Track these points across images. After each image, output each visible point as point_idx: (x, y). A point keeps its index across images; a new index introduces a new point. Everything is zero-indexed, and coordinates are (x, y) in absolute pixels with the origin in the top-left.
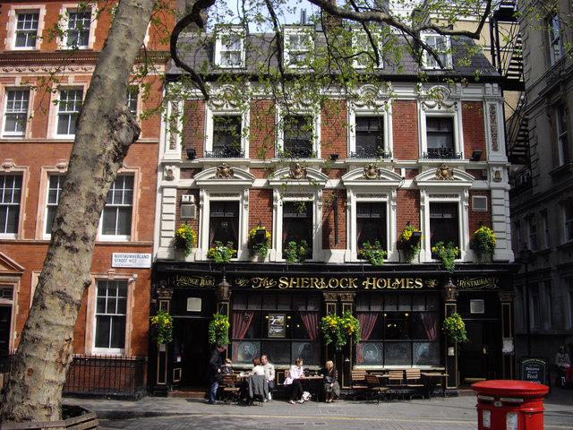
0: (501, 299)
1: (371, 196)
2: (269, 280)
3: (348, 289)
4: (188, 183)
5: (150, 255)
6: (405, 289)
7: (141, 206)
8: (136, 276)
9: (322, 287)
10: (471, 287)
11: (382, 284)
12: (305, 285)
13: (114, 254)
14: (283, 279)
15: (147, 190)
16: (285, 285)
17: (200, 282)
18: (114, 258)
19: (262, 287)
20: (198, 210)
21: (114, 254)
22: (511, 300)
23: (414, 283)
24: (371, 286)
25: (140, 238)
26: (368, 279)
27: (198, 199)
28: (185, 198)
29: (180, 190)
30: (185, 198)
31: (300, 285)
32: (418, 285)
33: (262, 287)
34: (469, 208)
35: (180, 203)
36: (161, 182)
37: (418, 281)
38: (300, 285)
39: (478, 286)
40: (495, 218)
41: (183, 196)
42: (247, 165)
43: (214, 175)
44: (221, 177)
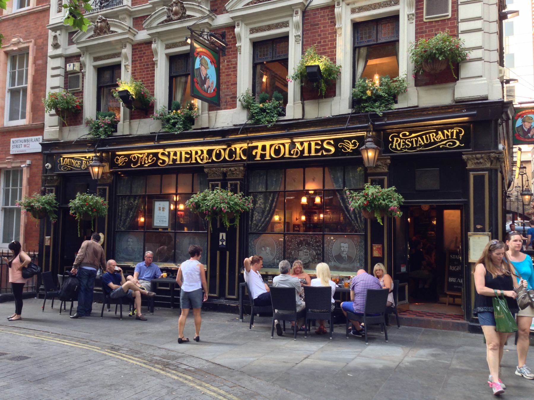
0: (470, 166)
1: (269, 28)
2: (148, 156)
3: (234, 161)
4: (73, 49)
5: (41, 137)
6: (309, 157)
7: (34, 83)
8: (28, 162)
9: (205, 161)
10: (412, 148)
11: (277, 152)
12: (187, 159)
13: (12, 140)
14: (163, 154)
15: (39, 65)
16: (164, 161)
17: (81, 164)
18: (12, 144)
19: (142, 166)
20: (83, 78)
21: (12, 140)
22: (488, 165)
23: (323, 148)
24: (263, 156)
25: (34, 119)
26: (260, 148)
27: (82, 66)
28: (70, 67)
29: (69, 59)
30: (70, 67)
31: (181, 160)
32: (328, 151)
33: (142, 166)
34: (418, 15)
35: (67, 74)
36: (51, 51)
37: (329, 143)
38: (181, 160)
39: (426, 145)
40: (462, 27)
41: (68, 65)
42: (129, 13)
43: (92, 33)
44: (99, 34)
